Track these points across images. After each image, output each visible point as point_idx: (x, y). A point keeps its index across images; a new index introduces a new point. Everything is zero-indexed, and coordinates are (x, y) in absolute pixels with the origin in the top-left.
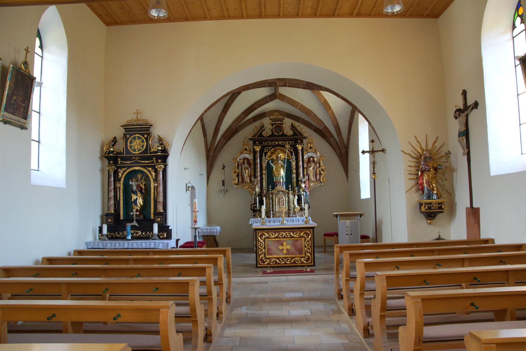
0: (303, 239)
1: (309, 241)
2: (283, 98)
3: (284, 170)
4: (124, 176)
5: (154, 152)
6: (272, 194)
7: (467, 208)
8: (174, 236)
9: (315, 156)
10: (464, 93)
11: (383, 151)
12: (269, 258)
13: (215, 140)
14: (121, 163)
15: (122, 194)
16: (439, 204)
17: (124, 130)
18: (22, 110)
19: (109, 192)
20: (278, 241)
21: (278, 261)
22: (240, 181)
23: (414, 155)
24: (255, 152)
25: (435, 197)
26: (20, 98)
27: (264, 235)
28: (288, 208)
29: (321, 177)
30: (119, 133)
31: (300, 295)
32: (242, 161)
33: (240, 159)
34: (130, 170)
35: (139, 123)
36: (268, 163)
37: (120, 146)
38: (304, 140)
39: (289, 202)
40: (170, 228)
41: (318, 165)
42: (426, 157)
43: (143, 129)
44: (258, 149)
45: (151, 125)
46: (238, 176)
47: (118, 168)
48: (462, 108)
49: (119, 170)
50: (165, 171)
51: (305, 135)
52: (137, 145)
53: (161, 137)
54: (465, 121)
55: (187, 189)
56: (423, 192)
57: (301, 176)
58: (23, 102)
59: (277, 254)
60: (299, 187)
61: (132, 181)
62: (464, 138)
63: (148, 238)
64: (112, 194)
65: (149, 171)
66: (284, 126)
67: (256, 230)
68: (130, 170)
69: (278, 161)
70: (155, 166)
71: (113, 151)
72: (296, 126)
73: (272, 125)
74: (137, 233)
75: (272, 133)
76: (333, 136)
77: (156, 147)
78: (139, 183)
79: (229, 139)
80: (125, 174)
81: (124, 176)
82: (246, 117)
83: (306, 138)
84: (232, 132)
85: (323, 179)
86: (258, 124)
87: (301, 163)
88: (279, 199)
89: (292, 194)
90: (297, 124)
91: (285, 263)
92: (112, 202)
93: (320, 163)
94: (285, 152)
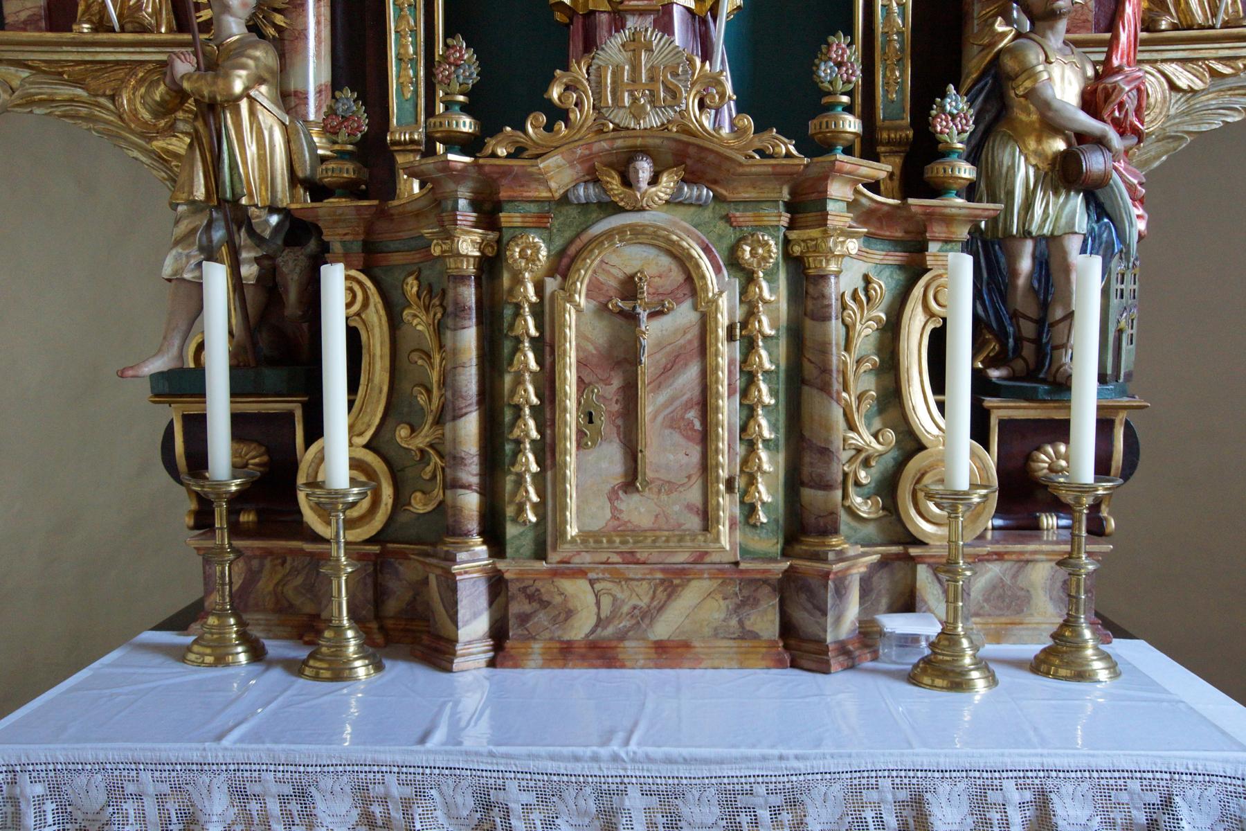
6: (488, 212)
28: (795, 481)
39: (805, 374)
88: (625, 305)
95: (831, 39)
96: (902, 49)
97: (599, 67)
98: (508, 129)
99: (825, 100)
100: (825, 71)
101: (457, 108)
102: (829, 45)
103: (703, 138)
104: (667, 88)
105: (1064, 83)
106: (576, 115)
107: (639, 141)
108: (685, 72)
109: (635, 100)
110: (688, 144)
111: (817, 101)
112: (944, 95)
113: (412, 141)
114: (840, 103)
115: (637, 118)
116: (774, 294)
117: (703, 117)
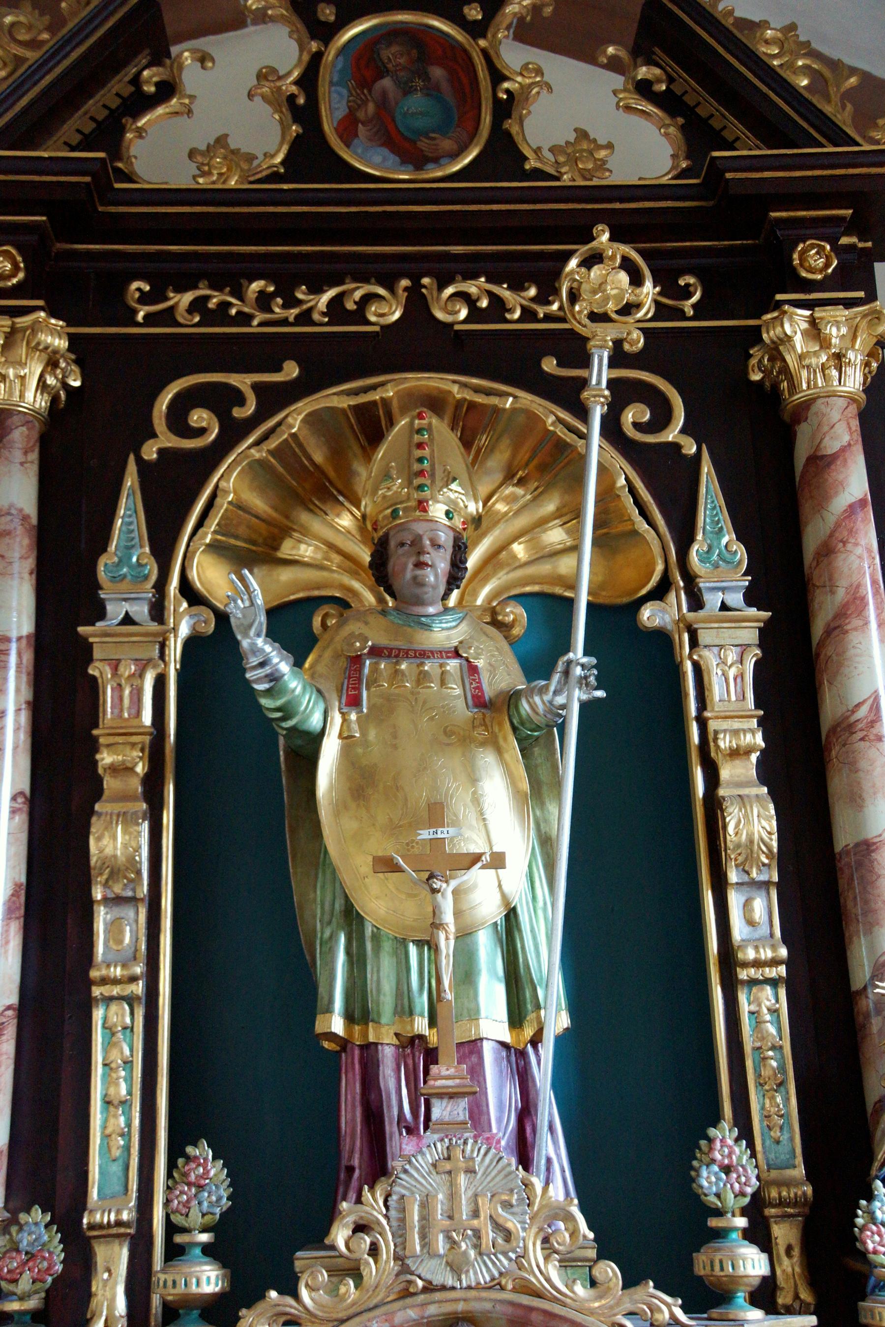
3: (537, 791)
36: (213, 656)
75: (310, 154)
94: (551, 466)
95: (712, 1132)
96: (782, 1068)
97: (403, 1197)
98: (273, 1294)
99: (713, 1222)
100: (708, 1180)
101: (198, 1251)
102: (711, 1141)
103: (555, 1300)
104: (498, 1227)
106: (370, 1269)
107: (460, 1307)
108: (520, 1200)
109: (453, 1244)
110: (531, 1309)
111: (698, 1224)
112: (870, 1197)
113: (119, 1223)
114: (735, 1229)
115: (456, 1269)
117: (550, 1267)
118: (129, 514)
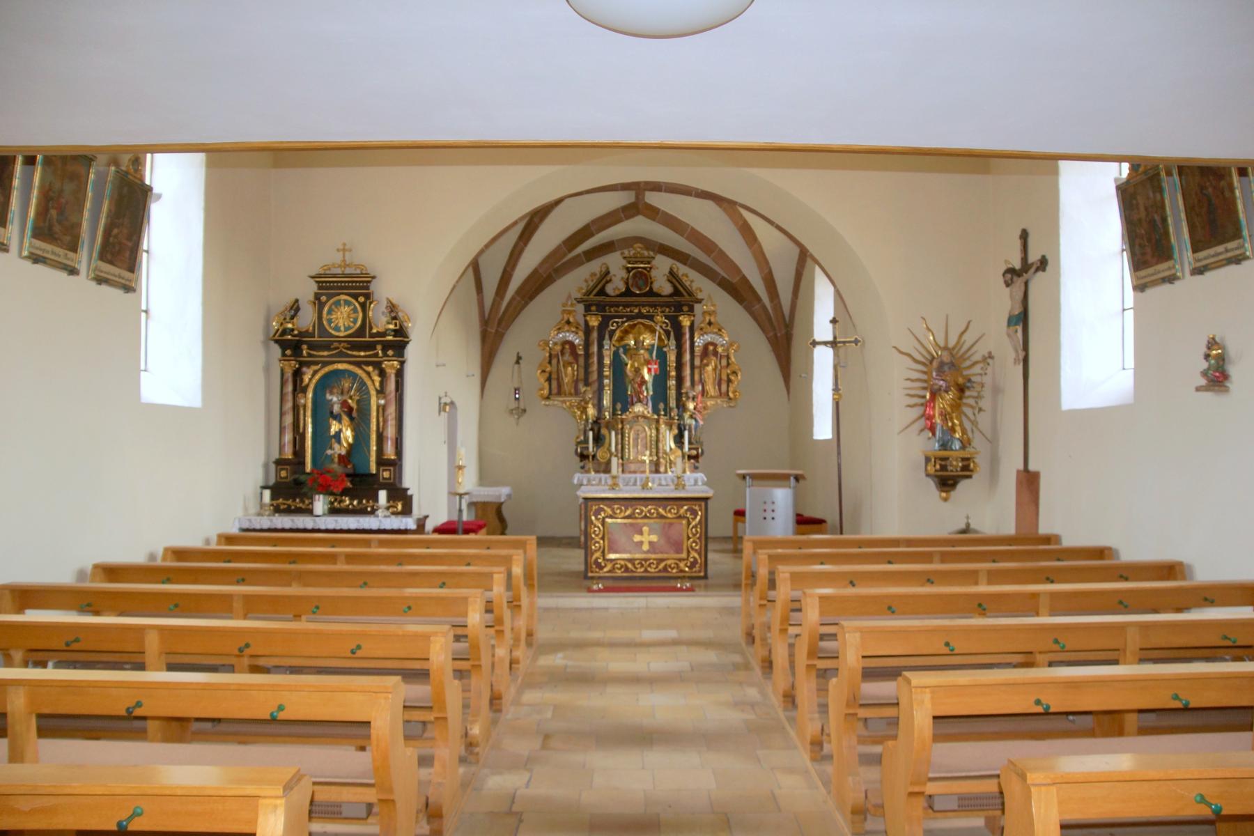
0: (684, 522)
1: (695, 527)
2: (653, 213)
4: (314, 381)
5: (379, 334)
7: (1018, 471)
8: (417, 511)
9: (718, 340)
10: (1024, 236)
11: (856, 342)
12: (611, 560)
13: (502, 298)
14: (310, 355)
15: (309, 420)
16: (963, 459)
17: (313, 287)
18: (127, 254)
19: (282, 414)
20: (631, 525)
21: (630, 566)
22: (555, 390)
23: (920, 358)
24: (588, 330)
25: (957, 445)
26: (125, 231)
27: (603, 510)
29: (731, 389)
30: (306, 291)
31: (672, 634)
32: (558, 348)
33: (555, 344)
34: (327, 369)
35: (348, 271)
36: (616, 354)
37: (306, 319)
38: (697, 306)
40: (409, 493)
41: (724, 362)
42: (942, 364)
43: (353, 286)
44: (594, 322)
45: (374, 277)
46: (549, 380)
47: (302, 364)
48: (1017, 265)
49: (304, 369)
50: (400, 374)
51: (700, 296)
52: (343, 319)
53: (394, 301)
54: (1021, 294)
55: (442, 407)
56: (934, 434)
57: (688, 383)
58: (129, 238)
59: (630, 552)
60: (681, 406)
61: (332, 393)
62: (1020, 329)
63: (362, 512)
64: (289, 419)
65: (368, 373)
66: (653, 273)
67: (586, 499)
68: (327, 369)
69: (637, 349)
70: (380, 363)
71: (292, 330)
72: (680, 274)
73: (628, 270)
74: (340, 502)
75: (628, 289)
76: (759, 299)
77: (381, 322)
78: (346, 397)
79: (532, 298)
80: (317, 377)
81: (314, 381)
82: (570, 251)
83: (699, 301)
84: (538, 283)
85: (734, 392)
86: (595, 266)
87: (687, 357)
89: (666, 424)
90: (682, 269)
91: (646, 571)
92: (288, 437)
93: (728, 357)
94: (653, 331)
105: (691, 406)
116: (654, 432)
118: (607, 337)
